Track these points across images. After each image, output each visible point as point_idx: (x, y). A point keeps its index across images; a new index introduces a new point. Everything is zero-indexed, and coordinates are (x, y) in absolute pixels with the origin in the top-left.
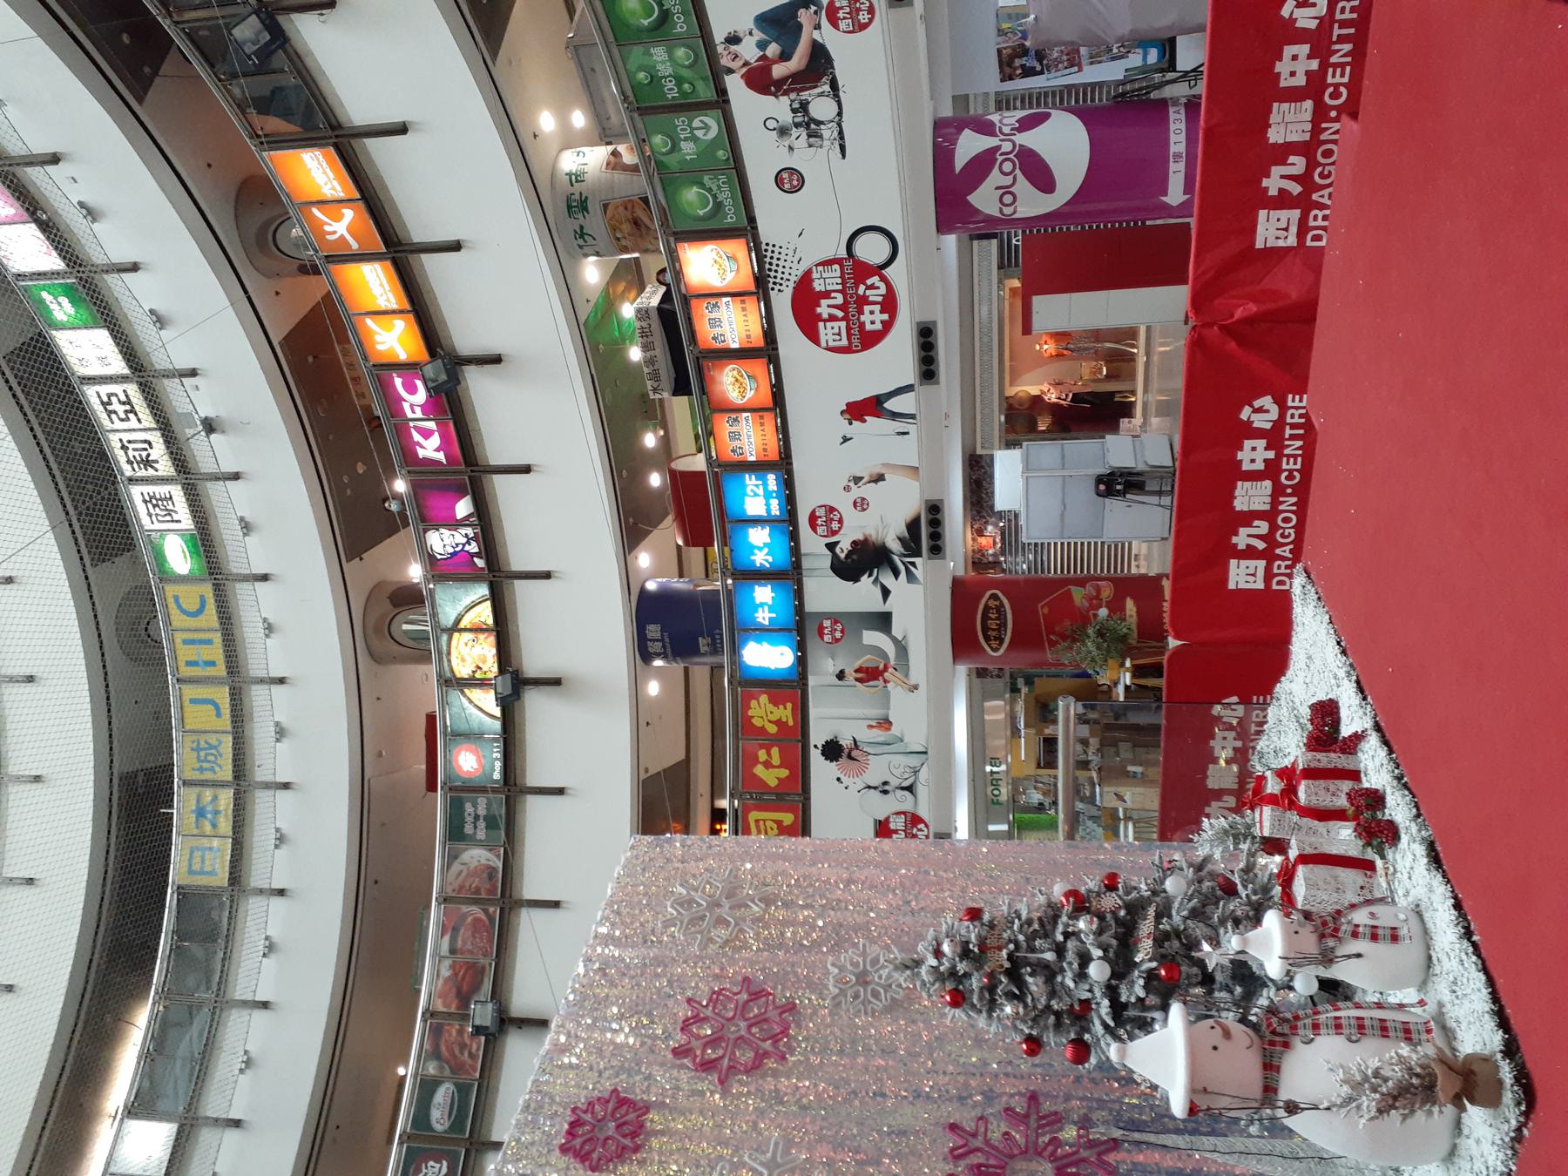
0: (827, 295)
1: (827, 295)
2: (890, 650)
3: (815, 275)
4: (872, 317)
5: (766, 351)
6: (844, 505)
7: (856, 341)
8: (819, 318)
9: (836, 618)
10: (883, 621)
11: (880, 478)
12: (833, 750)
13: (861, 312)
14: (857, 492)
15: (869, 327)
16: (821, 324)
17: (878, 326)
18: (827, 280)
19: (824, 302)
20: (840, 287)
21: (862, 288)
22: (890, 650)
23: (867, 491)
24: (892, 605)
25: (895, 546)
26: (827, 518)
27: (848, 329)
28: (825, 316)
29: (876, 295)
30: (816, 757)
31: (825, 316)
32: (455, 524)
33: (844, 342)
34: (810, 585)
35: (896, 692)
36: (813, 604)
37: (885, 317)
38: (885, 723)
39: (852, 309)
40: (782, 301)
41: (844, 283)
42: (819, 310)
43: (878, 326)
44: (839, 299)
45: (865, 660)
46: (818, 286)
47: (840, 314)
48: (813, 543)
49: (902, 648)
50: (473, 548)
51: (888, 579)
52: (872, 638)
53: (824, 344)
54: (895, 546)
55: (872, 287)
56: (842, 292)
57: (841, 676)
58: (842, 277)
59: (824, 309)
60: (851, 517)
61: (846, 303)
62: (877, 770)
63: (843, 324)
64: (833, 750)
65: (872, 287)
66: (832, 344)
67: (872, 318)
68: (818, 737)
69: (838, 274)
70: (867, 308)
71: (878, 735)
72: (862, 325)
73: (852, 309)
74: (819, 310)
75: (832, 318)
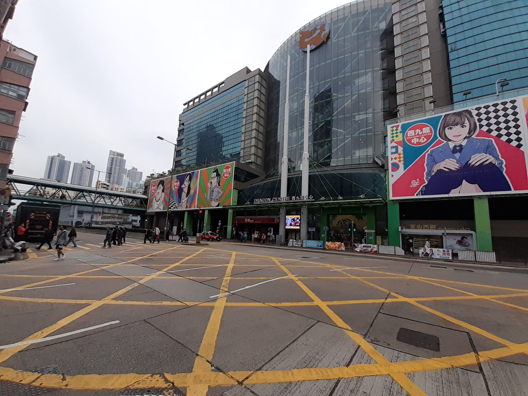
0: (422, 131)
1: (422, 131)
3: (427, 128)
4: (415, 141)
7: (410, 138)
13: (417, 138)
15: (412, 140)
16: (414, 130)
17: (413, 142)
19: (420, 131)
20: (423, 133)
21: (423, 137)
27: (412, 136)
28: (416, 131)
29: (421, 140)
33: (408, 136)
37: (415, 143)
41: (425, 134)
42: (417, 130)
43: (413, 142)
55: (423, 139)
56: (422, 134)
61: (420, 135)
65: (423, 139)
66: (408, 133)
69: (427, 132)
70: (418, 139)
72: (413, 139)
75: (415, 133)
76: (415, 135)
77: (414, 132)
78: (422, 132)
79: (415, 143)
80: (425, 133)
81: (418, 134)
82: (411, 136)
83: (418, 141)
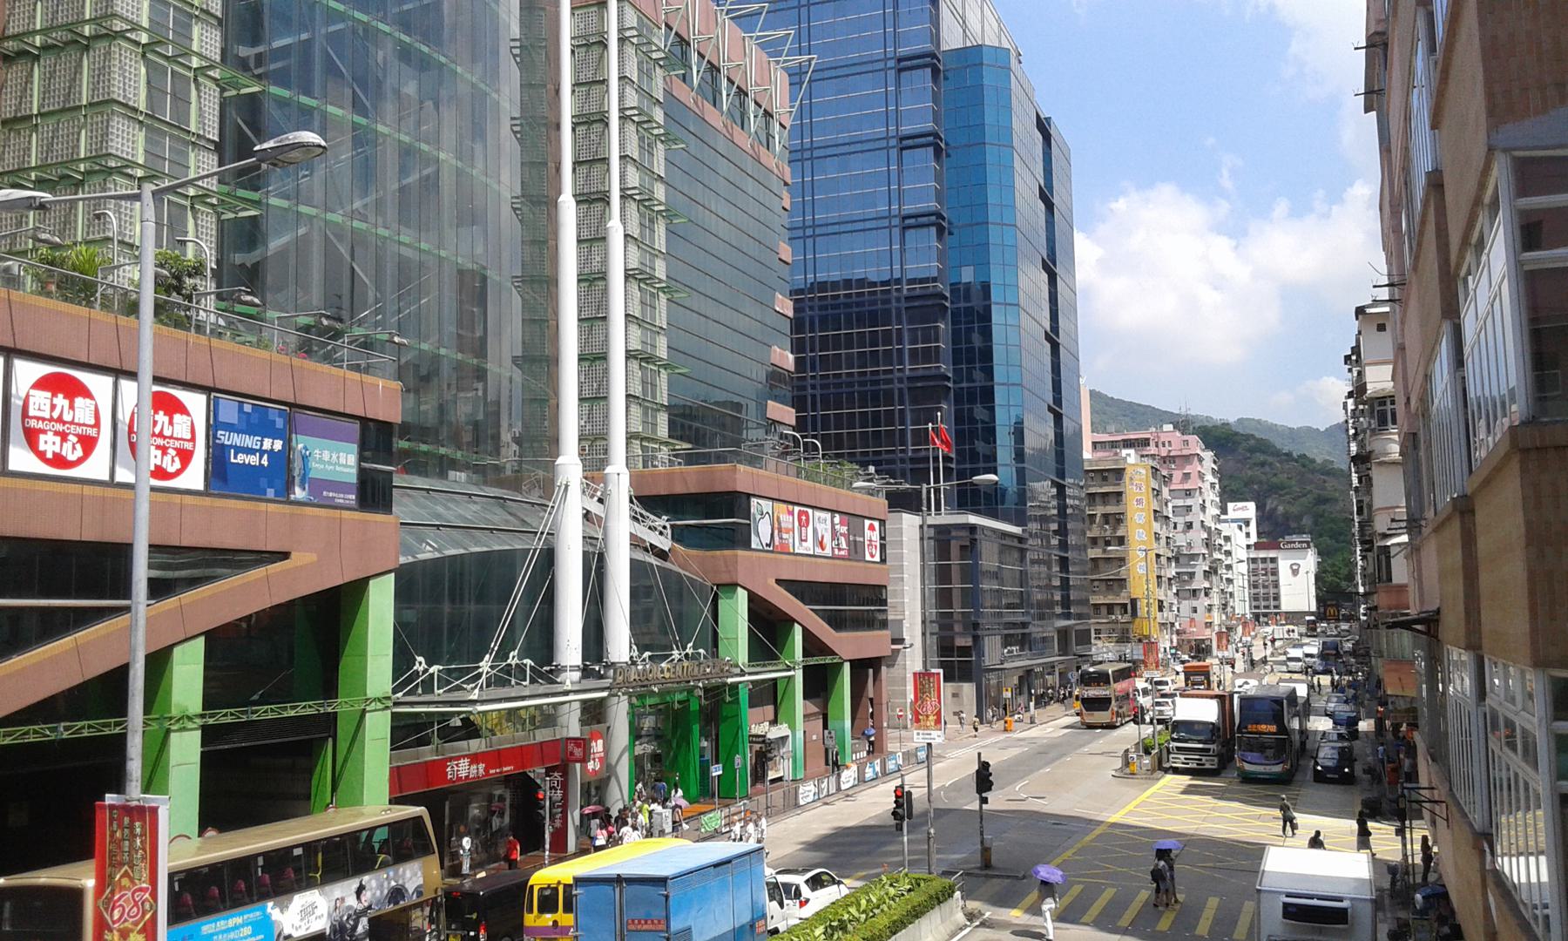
0: (72, 407)
1: (72, 407)
3: (88, 400)
4: (50, 443)
8: (54, 395)
13: (56, 433)
15: (42, 438)
16: (49, 395)
27: (44, 419)
28: (55, 401)
31: (55, 401)
33: (32, 413)
37: (49, 455)
39: (59, 427)
41: (79, 425)
42: (61, 396)
43: (42, 447)
44: (67, 417)
46: (79, 401)
47: (56, 415)
53: (32, 392)
56: (72, 423)
58: (84, 425)
59: (60, 400)
61: (64, 423)
63: (47, 416)
65: (74, 448)
66: (31, 400)
70: (58, 439)
72: (44, 432)
73: (59, 427)
74: (61, 396)
75: (53, 407)
76: (51, 419)
77: (48, 402)
78: (71, 412)
79: (49, 455)
80: (82, 422)
81: (60, 420)
82: (38, 418)
83: (58, 450)
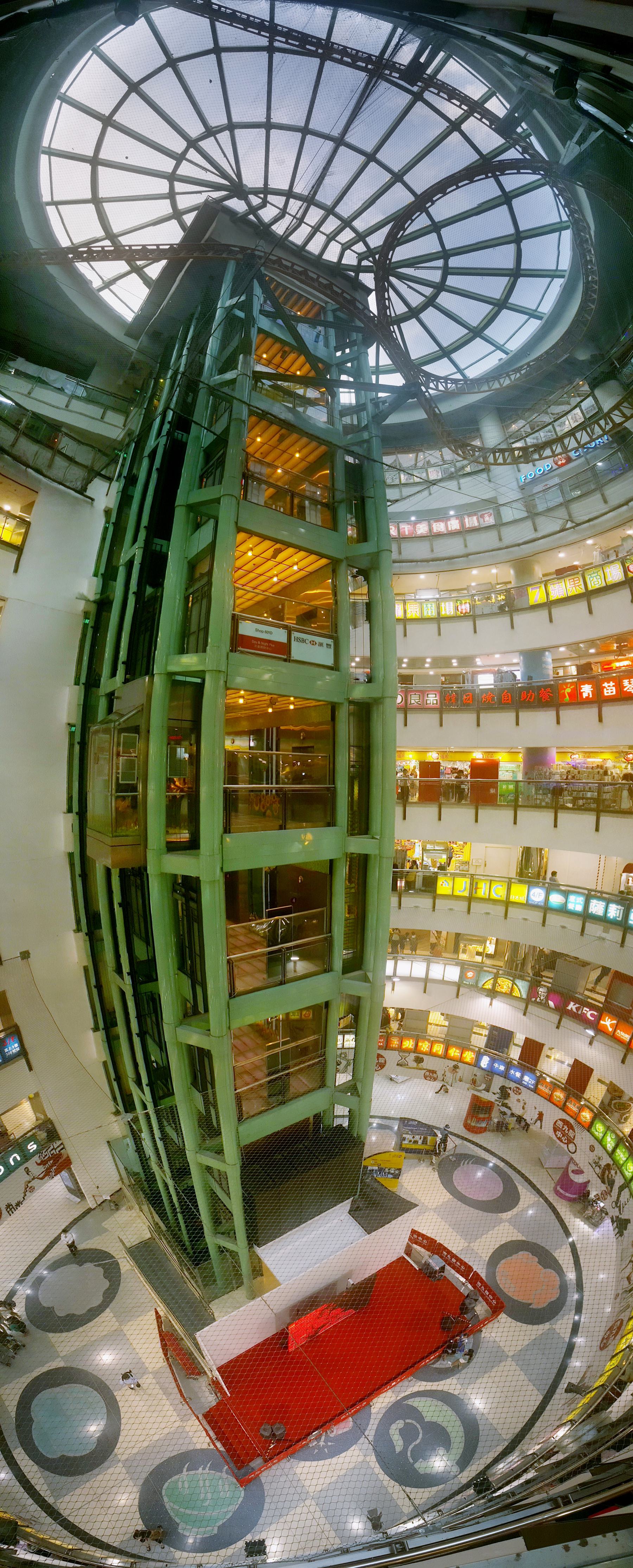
2: (481, 1088)
5: (564, 1108)
6: (519, 1097)
9: (491, 1080)
10: (487, 1090)
11: (523, 1108)
12: (456, 1067)
14: (522, 1102)
18: (571, 1132)
22: (481, 1088)
23: (522, 1104)
24: (490, 1094)
25: (506, 1101)
26: (518, 1091)
29: (563, 1138)
30: (455, 1063)
32: (547, 998)
34: (502, 1079)
35: (468, 1086)
36: (496, 1077)
38: (461, 1080)
40: (572, 1121)
45: (478, 1082)
48: (513, 1085)
49: (479, 1091)
50: (538, 1000)
51: (497, 1096)
52: (483, 1086)
54: (506, 1101)
57: (475, 1075)
59: (566, 1127)
60: (517, 1097)
62: (449, 1075)
64: (456, 1067)
67: (559, 1134)
68: (460, 1064)
71: (458, 1078)
